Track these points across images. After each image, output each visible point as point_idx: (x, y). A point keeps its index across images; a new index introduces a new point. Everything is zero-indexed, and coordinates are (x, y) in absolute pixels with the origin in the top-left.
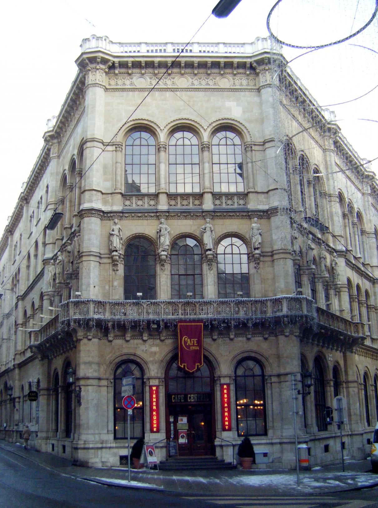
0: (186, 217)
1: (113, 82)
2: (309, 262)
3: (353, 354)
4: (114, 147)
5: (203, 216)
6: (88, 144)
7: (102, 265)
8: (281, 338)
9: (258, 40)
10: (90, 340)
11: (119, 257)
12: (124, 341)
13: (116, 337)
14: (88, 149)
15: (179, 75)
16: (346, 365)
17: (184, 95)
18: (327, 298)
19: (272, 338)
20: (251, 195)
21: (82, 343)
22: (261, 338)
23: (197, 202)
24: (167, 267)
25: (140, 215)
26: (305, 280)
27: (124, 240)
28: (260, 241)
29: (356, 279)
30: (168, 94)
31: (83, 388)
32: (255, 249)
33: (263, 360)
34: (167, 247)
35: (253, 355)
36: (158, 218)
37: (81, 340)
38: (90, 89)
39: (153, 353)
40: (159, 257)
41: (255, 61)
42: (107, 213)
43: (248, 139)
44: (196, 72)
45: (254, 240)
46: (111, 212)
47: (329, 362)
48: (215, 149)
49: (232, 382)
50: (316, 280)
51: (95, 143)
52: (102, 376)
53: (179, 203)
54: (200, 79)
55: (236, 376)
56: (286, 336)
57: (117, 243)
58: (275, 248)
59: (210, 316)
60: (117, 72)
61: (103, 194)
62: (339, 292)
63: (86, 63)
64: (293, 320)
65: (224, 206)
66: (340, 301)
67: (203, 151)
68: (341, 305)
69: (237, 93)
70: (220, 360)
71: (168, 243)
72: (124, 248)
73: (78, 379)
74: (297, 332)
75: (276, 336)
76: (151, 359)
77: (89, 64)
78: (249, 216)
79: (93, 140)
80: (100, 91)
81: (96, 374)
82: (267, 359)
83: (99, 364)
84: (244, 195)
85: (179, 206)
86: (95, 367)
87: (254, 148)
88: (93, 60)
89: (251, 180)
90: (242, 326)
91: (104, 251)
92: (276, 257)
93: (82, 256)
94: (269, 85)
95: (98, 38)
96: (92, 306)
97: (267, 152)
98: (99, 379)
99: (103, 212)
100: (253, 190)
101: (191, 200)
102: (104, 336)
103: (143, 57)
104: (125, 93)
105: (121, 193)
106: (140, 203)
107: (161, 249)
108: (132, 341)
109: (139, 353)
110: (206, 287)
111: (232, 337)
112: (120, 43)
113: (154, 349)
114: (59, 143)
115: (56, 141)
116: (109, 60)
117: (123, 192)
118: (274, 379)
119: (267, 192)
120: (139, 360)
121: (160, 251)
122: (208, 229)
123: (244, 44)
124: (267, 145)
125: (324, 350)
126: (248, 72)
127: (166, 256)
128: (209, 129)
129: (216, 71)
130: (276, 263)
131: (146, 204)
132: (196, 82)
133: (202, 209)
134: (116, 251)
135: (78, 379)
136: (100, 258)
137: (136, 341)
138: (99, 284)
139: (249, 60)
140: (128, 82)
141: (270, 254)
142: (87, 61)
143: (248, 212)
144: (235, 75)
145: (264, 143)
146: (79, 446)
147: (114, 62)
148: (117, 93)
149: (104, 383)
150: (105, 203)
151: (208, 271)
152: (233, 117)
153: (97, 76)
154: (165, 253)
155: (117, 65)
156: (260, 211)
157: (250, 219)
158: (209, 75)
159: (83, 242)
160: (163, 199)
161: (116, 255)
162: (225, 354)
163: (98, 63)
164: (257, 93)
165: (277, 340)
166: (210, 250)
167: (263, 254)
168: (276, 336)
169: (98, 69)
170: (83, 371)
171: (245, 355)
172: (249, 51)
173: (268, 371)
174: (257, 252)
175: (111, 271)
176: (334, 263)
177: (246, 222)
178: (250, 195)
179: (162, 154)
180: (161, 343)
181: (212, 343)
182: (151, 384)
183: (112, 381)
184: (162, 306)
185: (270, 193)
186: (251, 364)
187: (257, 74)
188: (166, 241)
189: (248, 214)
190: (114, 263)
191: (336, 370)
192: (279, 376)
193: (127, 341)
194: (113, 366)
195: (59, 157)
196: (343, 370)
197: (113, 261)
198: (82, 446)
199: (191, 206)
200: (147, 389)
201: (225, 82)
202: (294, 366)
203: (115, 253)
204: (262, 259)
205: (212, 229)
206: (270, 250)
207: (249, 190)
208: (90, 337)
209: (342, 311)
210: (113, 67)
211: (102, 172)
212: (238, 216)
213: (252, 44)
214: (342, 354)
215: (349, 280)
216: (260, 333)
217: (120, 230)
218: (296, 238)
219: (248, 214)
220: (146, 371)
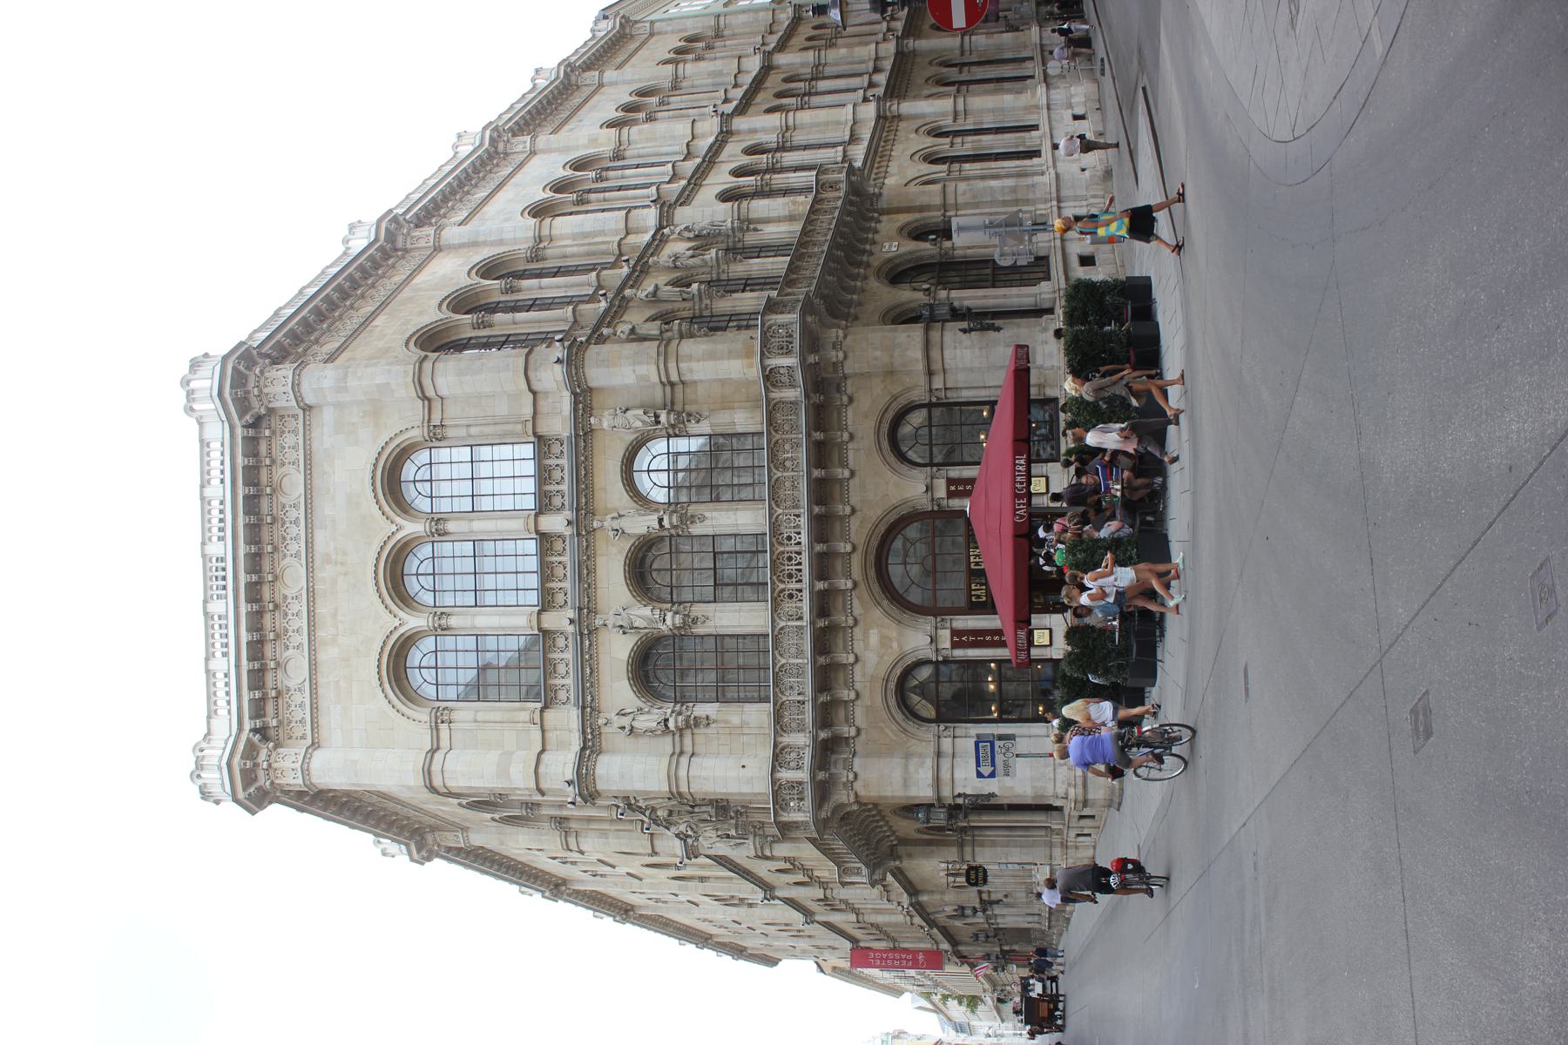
0: (591, 571)
1: (298, 732)
3: (885, 191)
4: (442, 726)
5: (588, 533)
6: (437, 782)
8: (849, 368)
9: (192, 409)
11: (680, 713)
12: (858, 703)
13: (849, 721)
14: (448, 784)
15: (278, 584)
16: (908, 210)
17: (324, 573)
18: (761, 251)
19: (850, 387)
20: (542, 430)
21: (862, 793)
22: (850, 410)
23: (558, 545)
24: (698, 610)
26: (724, 305)
27: (641, 705)
28: (641, 412)
29: (721, 178)
30: (322, 610)
31: (958, 790)
32: (658, 422)
33: (896, 407)
35: (885, 427)
37: (856, 795)
38: (314, 780)
39: (883, 642)
40: (679, 628)
42: (585, 740)
43: (416, 434)
44: (269, 549)
45: (638, 424)
46: (584, 732)
47: (903, 250)
48: (444, 506)
49: (943, 473)
50: (724, 277)
51: (433, 768)
52: (931, 748)
53: (560, 585)
55: (931, 464)
56: (845, 357)
57: (648, 721)
58: (655, 379)
59: (804, 521)
61: (543, 750)
62: (750, 221)
63: (256, 792)
64: (812, 342)
65: (565, 487)
66: (767, 221)
67: (446, 533)
68: (778, 219)
71: (647, 611)
72: (659, 704)
73: (939, 799)
74: (835, 334)
75: (845, 377)
76: (895, 645)
77: (257, 784)
79: (428, 773)
80: (319, 759)
81: (929, 762)
82: (895, 398)
83: (908, 756)
84: (542, 444)
85: (567, 585)
86: (914, 761)
87: (436, 421)
88: (249, 777)
89: (509, 427)
90: (822, 453)
91: (666, 744)
92: (674, 377)
93: (680, 794)
94: (296, 386)
95: (199, 766)
96: (785, 775)
97: (444, 392)
98: (939, 754)
99: (583, 749)
100: (530, 425)
101: (554, 559)
102: (848, 745)
103: (238, 666)
104: (323, 704)
105: (542, 711)
106: (561, 669)
107: (660, 625)
108: (858, 686)
109: (882, 673)
111: (847, 473)
112: (209, 717)
113: (874, 638)
114: (434, 829)
115: (429, 838)
116: (248, 740)
117: (539, 705)
118: (938, 383)
119: (534, 393)
120: (898, 671)
121: (664, 628)
122: (616, 525)
123: (202, 441)
124: (430, 393)
125: (875, 262)
126: (267, 433)
127: (676, 613)
128: (398, 520)
129: (265, 503)
131: (565, 656)
132: (293, 547)
133: (572, 536)
134: (666, 720)
135: (939, 799)
136: (681, 753)
137: (857, 677)
138: (736, 756)
139: (239, 431)
140: (297, 698)
141: (668, 389)
142: (252, 790)
143: (577, 435)
144: (273, 462)
145: (424, 397)
146: (1080, 798)
148: (323, 721)
149: (946, 743)
152: (370, 467)
153: (288, 766)
154: (669, 615)
155: (259, 724)
156: (575, 410)
158: (274, 520)
159: (647, 793)
160: (553, 620)
162: (883, 488)
163: (256, 765)
164: (314, 411)
166: (661, 520)
167: (670, 406)
168: (845, 377)
169: (270, 765)
170: (923, 790)
171: (885, 444)
172: (217, 432)
173: (919, 394)
174: (663, 418)
175: (708, 731)
176: (687, 234)
177: (599, 442)
178: (540, 431)
179: (453, 621)
180: (861, 624)
182: (948, 645)
183: (942, 727)
184: (782, 624)
185: (535, 387)
186: (905, 430)
187: (271, 411)
188: (643, 614)
189: (583, 435)
190: (694, 724)
191: (919, 234)
192: (930, 373)
194: (911, 726)
195: (464, 829)
196: (917, 216)
197: (688, 726)
198: (1080, 790)
199: (566, 559)
200: (959, 653)
201: (293, 483)
202: (910, 339)
203: (671, 724)
204: (678, 407)
206: (659, 389)
207: (530, 432)
208: (851, 776)
209: (791, 218)
210: (262, 732)
211: (497, 751)
213: (201, 424)
214: (884, 218)
215: (726, 196)
216: (839, 413)
217: (621, 714)
218: (633, 330)
219: (583, 435)
220: (921, 655)
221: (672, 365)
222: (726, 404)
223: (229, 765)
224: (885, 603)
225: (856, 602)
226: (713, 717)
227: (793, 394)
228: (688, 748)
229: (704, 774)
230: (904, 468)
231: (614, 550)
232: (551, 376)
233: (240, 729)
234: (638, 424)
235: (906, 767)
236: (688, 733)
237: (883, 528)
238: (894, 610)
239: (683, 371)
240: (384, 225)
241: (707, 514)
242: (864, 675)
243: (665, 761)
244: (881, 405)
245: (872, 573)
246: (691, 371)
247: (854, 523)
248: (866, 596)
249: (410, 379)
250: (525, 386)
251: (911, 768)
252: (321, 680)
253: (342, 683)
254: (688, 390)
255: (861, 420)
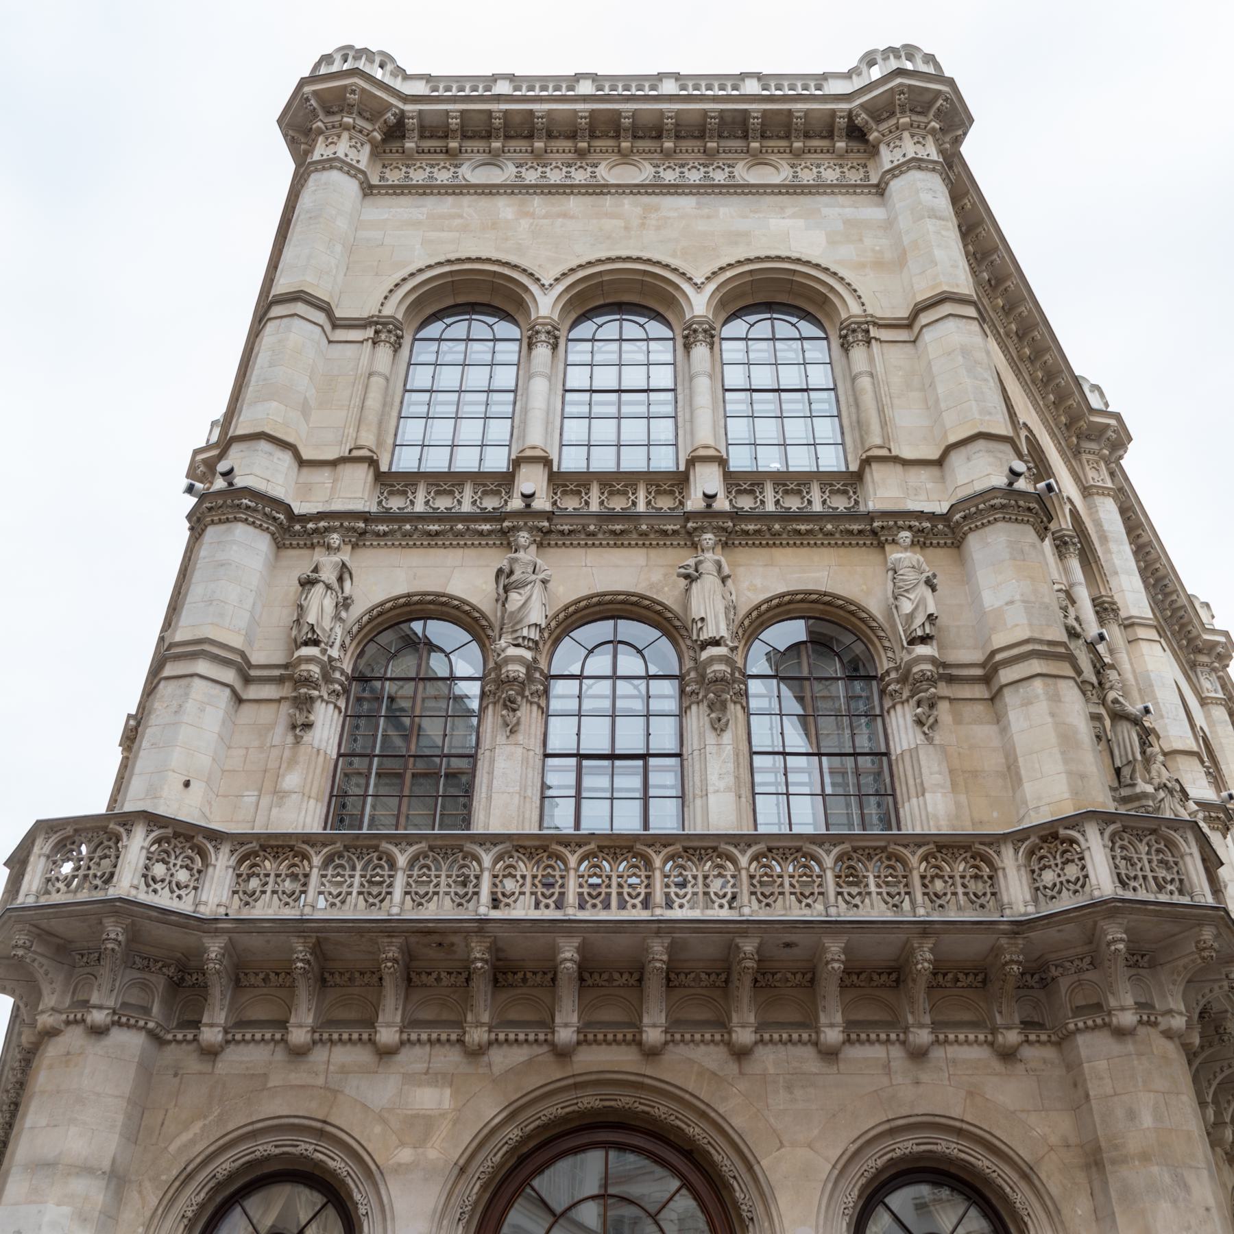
2: (1126, 772)
7: (246, 708)
8: (1094, 1049)
10: (98, 1032)
17: (628, 204)
25: (434, 527)
28: (931, 609)
30: (574, 204)
32: (912, 642)
34: (534, 634)
36: (505, 539)
41: (861, 105)
42: (304, 519)
45: (907, 607)
54: (682, 166)
58: (999, 641)
60: (410, 145)
61: (302, 463)
67: (687, 347)
69: (803, 199)
70: (777, 1165)
78: (874, 533)
80: (351, 187)
82: (1027, 1175)
84: (853, 480)
87: (874, 332)
89: (875, 427)
92: (1006, 675)
94: (917, 163)
97: (928, 335)
100: (884, 452)
110: (698, 802)
119: (939, 463)
124: (924, 319)
130: (1009, 697)
134: (316, 643)
137: (342, 1056)
141: (979, 672)
147: (402, 112)
150: (305, 491)
151: (711, 737)
156: (920, 515)
157: (881, 546)
161: (309, 660)
164: (876, 199)
165: (1073, 1068)
166: (716, 642)
179: (542, 352)
181: (733, 1068)
187: (873, 151)
189: (874, 532)
193: (298, 1053)
204: (943, 689)
205: (726, 571)
206: (979, 657)
210: (396, 131)
212: (831, 534)
216: (974, 1025)
217: (344, 572)
219: (874, 532)
221: (1036, 666)
222: (961, 778)
223: (355, 72)
224: (513, 1133)
225: (519, 1055)
226: (308, 737)
227: (1017, 893)
228: (253, 692)
229: (190, 706)
230: (850, 1195)
231: (657, 576)
232: (982, 472)
233: (406, 99)
234: (907, 607)
235: (86, 1170)
236: (286, 690)
237: (696, 1131)
238: (493, 1157)
239: (1022, 689)
240: (1113, 422)
241: (727, 737)
242: (344, 1070)
243: (237, 642)
244: (1004, 1133)
245: (589, 1101)
246: (1027, 703)
247: (710, 1057)
248: (534, 1081)
249: (946, 288)
250: (952, 439)
251: (79, 1185)
252: (466, 200)
253: (459, 221)
254: (979, 708)
255: (970, 1086)
